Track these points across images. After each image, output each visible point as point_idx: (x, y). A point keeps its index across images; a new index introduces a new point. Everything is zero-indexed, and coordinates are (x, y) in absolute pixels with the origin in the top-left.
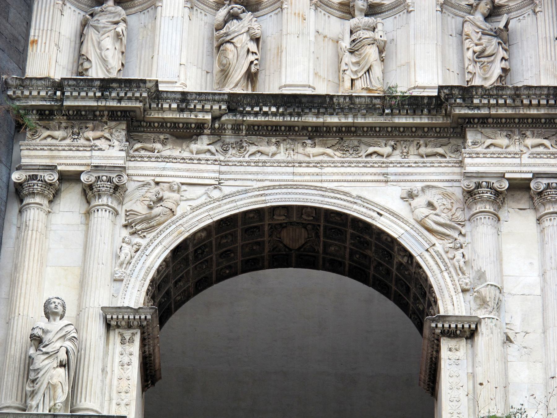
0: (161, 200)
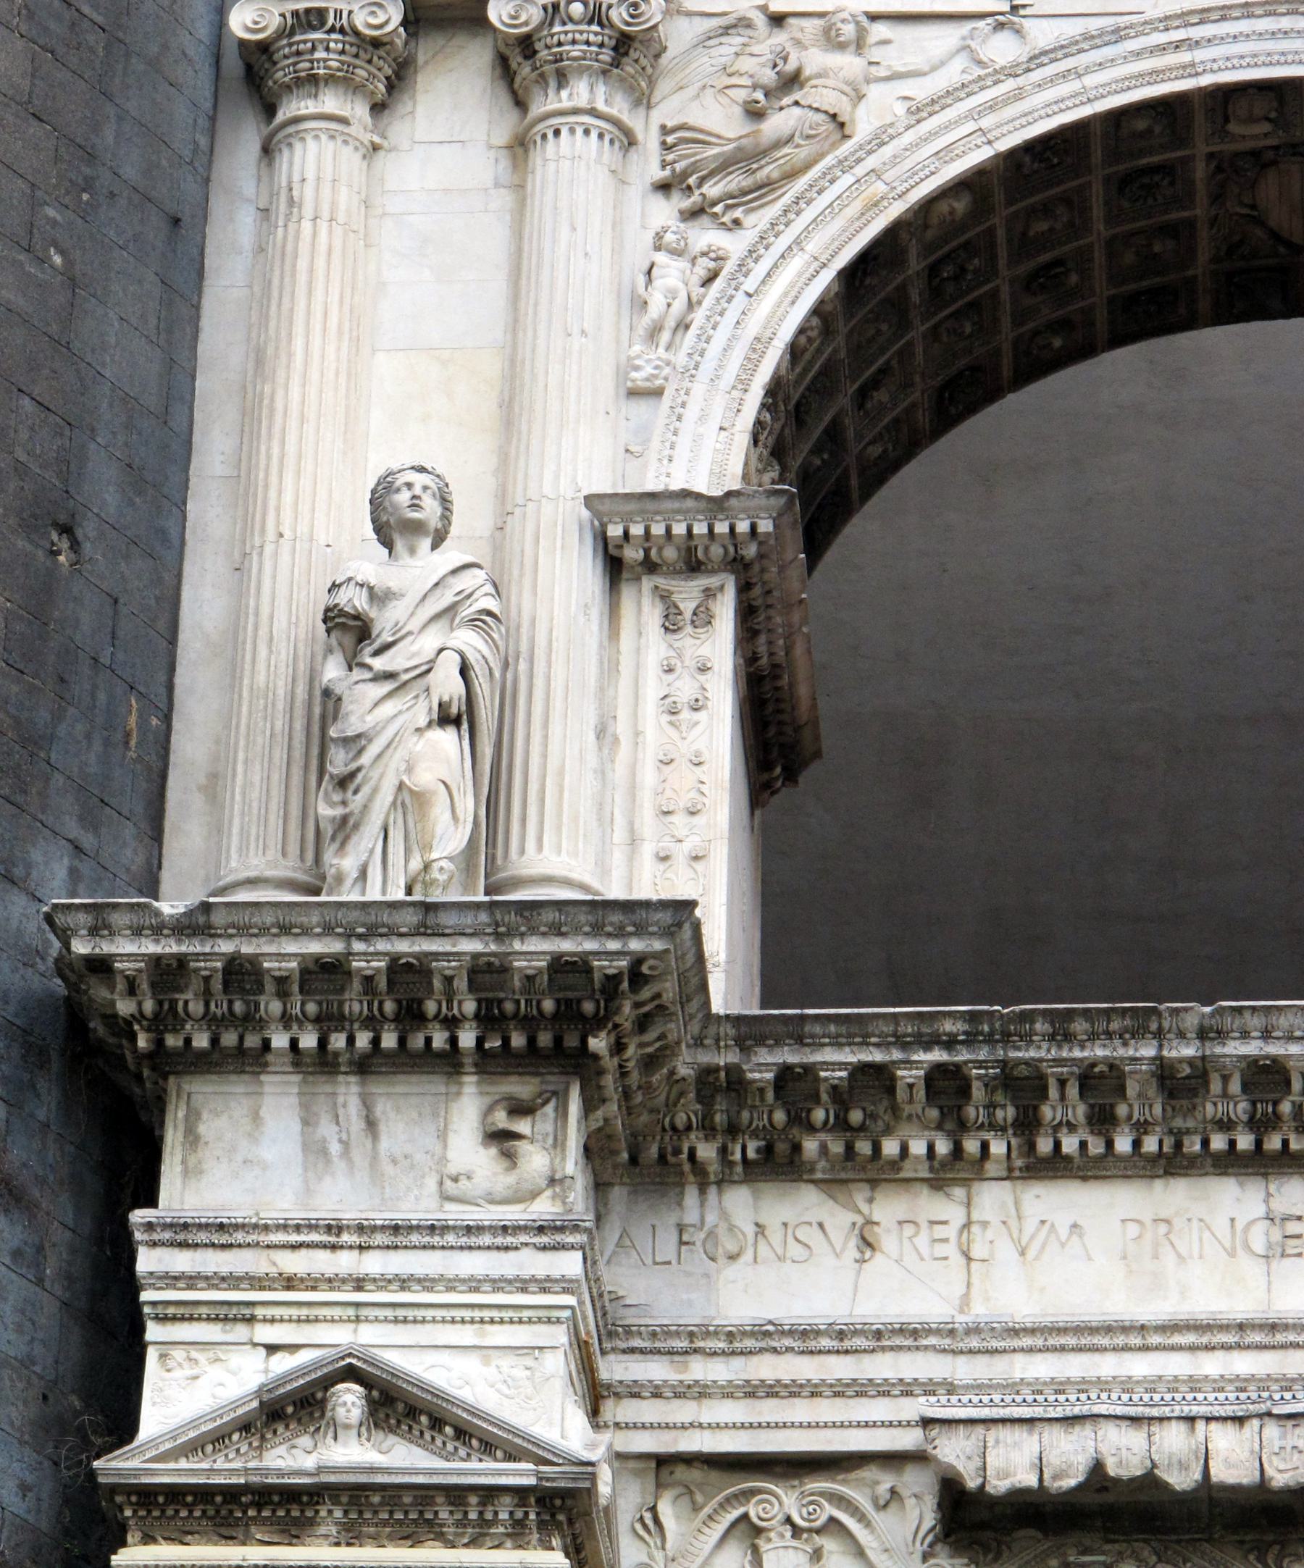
0: (792, 81)
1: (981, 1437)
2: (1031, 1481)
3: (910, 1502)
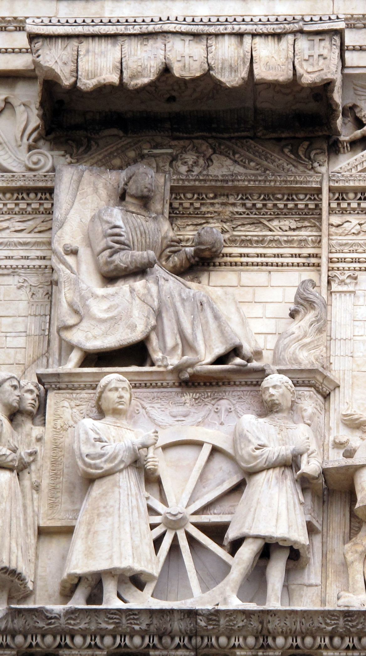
1: (76, 48)
2: (114, 79)
3: (20, 109)
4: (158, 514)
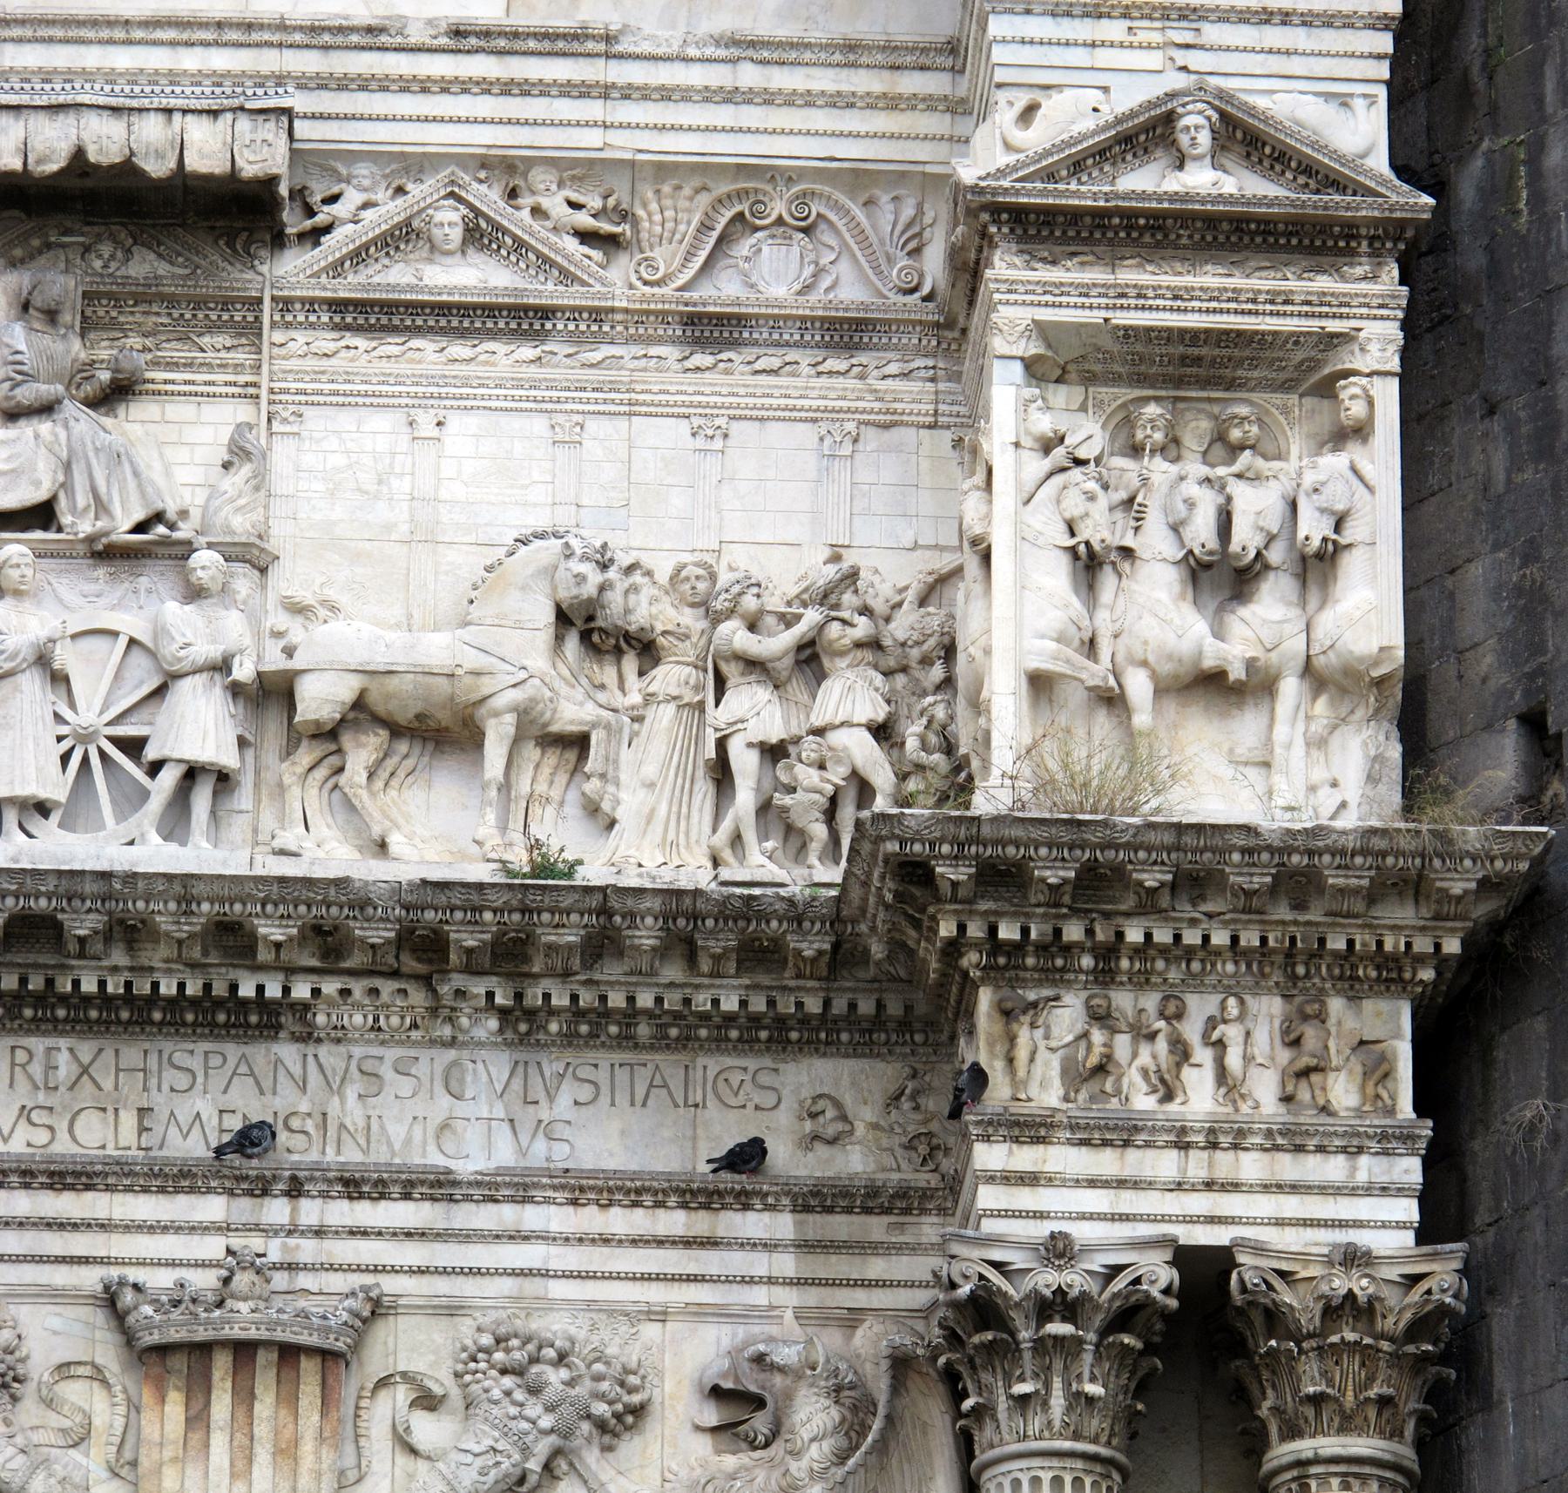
2: (16, 164)
4: (66, 723)
